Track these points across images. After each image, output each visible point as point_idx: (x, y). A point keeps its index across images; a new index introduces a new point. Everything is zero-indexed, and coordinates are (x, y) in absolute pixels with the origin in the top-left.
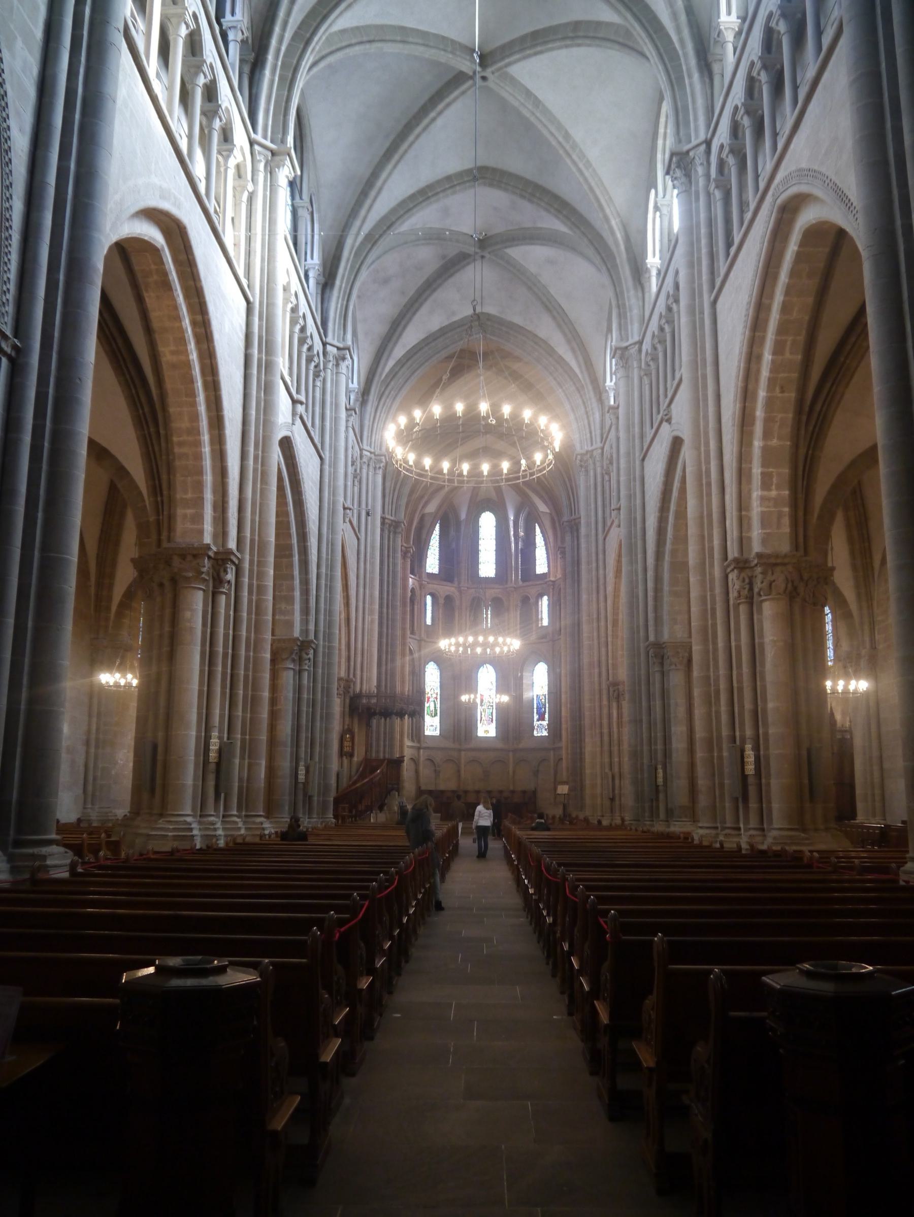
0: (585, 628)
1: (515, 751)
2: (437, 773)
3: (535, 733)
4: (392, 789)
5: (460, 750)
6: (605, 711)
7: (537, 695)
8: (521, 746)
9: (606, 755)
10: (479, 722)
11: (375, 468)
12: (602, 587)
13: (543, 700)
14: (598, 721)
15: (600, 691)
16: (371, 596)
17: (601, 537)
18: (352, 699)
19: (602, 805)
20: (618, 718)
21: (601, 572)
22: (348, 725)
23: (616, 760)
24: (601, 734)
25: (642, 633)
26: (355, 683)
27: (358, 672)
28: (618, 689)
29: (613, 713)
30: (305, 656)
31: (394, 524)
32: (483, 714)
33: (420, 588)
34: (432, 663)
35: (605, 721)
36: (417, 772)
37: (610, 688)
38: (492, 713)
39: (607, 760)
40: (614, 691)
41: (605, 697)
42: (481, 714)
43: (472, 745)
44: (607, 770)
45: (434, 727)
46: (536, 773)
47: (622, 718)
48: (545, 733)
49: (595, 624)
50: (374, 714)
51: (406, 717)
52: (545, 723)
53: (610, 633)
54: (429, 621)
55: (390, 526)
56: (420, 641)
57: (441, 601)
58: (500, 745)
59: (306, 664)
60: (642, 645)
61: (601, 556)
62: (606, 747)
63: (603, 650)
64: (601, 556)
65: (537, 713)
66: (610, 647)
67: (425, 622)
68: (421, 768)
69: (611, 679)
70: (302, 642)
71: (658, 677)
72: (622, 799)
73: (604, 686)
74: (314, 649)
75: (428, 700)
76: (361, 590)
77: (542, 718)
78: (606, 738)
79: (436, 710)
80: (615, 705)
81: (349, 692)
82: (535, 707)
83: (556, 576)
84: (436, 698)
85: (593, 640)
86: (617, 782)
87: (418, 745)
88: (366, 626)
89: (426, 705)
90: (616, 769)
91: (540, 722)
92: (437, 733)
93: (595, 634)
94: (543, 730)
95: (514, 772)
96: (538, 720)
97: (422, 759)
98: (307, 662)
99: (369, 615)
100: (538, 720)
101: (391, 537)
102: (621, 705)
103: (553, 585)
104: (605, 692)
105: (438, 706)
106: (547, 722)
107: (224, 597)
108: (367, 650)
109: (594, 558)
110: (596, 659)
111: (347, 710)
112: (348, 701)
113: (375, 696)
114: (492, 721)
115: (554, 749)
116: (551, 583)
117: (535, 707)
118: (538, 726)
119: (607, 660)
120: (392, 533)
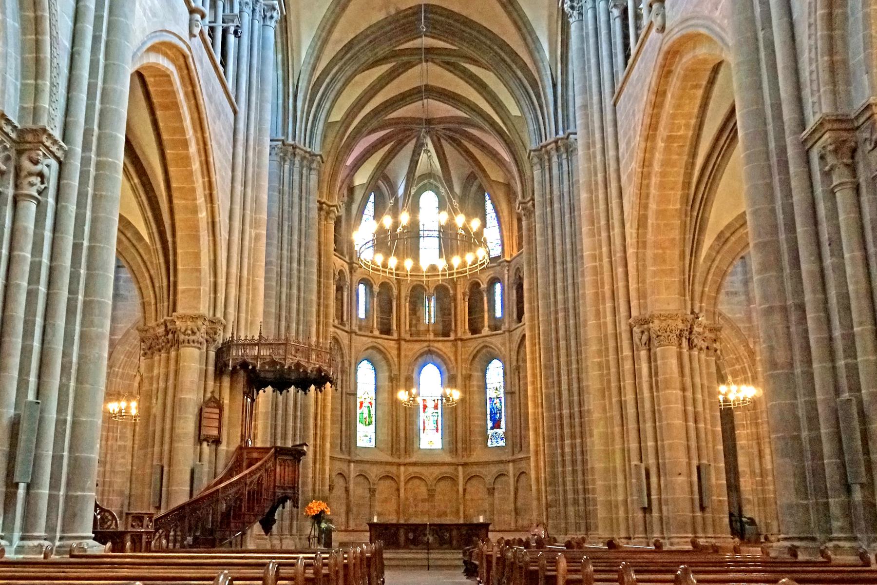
0: (586, 242)
1: (465, 465)
2: (372, 491)
3: (489, 444)
4: (283, 501)
5: (399, 465)
6: (627, 366)
7: (491, 398)
8: (472, 459)
9: (633, 435)
10: (422, 431)
11: (265, 17)
12: (613, 176)
13: (498, 405)
14: (614, 384)
15: (616, 336)
16: (256, 200)
17: (608, 102)
18: (219, 353)
19: (627, 519)
20: (650, 376)
21: (611, 153)
22: (213, 392)
23: (650, 443)
24: (622, 405)
25: (788, 114)
26: (225, 327)
27: (232, 310)
28: (649, 330)
29: (640, 369)
30: (27, 165)
31: (307, 155)
32: (426, 422)
33: (351, 272)
34: (366, 361)
35: (628, 382)
36: (347, 490)
37: (635, 329)
38: (437, 421)
39: (634, 446)
40: (643, 332)
41: (626, 344)
42: (424, 423)
43: (413, 459)
44: (635, 462)
45: (368, 438)
46: (491, 491)
47: (657, 374)
48: (502, 443)
49: (604, 234)
50: (262, 384)
51: (313, 387)
52: (501, 431)
53: (630, 240)
54: (362, 314)
55: (303, 158)
56: (351, 332)
57: (376, 289)
58: (448, 459)
59: (32, 185)
60: (789, 140)
61: (609, 130)
62: (632, 425)
63: (620, 270)
64: (609, 130)
65: (491, 420)
66: (631, 264)
67: (357, 315)
68: (352, 487)
69: (635, 313)
70: (22, 133)
71: (843, 198)
72: (664, 508)
73: (623, 327)
74: (60, 163)
75: (361, 407)
76: (239, 188)
77: (496, 425)
78: (631, 411)
79: (370, 417)
80: (643, 353)
81: (214, 341)
82: (489, 412)
83: (511, 255)
84: (370, 403)
85: (601, 260)
86: (654, 479)
87: (348, 458)
88: (246, 243)
89: (359, 411)
90: (652, 461)
91: (495, 430)
92: (372, 444)
93: (605, 249)
94: (499, 440)
95: (465, 490)
96: (492, 428)
97: (352, 475)
98: (36, 180)
99: (251, 227)
100: (492, 428)
101: (304, 172)
102: (655, 354)
103: (508, 266)
104: (625, 336)
105: (373, 412)
106: (504, 430)
107: (33, 206)
108: (248, 280)
109: (598, 135)
110: (607, 288)
111: (211, 368)
112: (212, 354)
113: (255, 345)
114: (437, 430)
115: (514, 461)
116: (506, 264)
117: (489, 412)
118: (492, 436)
119: (627, 287)
120: (305, 169)
